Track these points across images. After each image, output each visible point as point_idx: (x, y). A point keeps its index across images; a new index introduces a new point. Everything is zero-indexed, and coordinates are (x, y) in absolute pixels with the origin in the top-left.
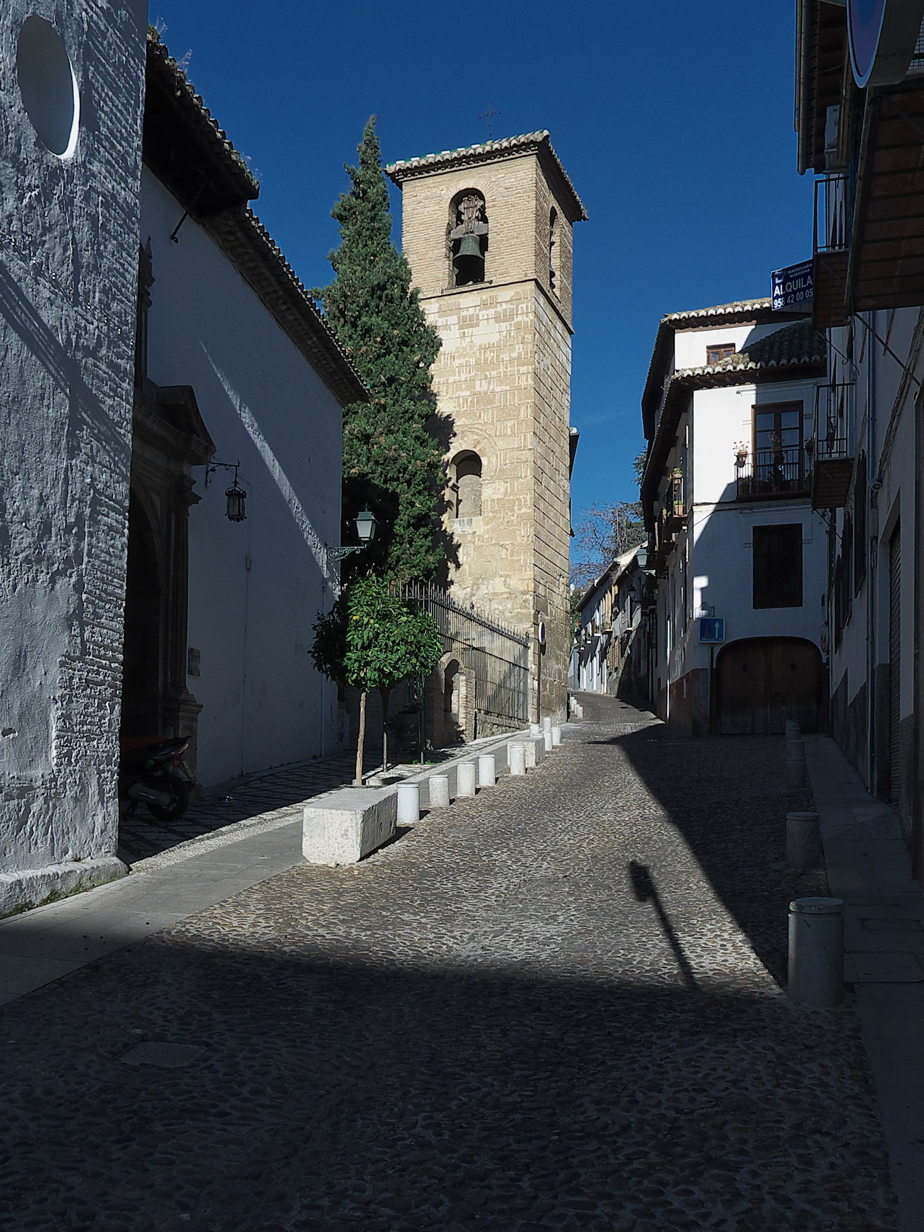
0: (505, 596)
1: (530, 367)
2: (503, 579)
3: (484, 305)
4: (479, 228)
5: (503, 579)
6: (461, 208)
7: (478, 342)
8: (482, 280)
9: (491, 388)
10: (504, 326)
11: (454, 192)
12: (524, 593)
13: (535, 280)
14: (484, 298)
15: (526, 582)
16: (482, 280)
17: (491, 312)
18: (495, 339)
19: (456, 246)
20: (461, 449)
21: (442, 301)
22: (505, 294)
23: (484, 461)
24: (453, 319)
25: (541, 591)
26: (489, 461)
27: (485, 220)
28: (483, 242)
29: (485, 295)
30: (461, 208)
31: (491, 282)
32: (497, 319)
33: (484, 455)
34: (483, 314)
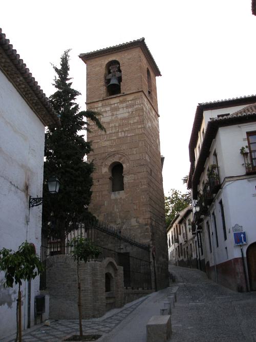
0: (137, 227)
2: (135, 219)
3: (121, 102)
4: (118, 74)
5: (135, 219)
6: (110, 68)
7: (119, 116)
8: (120, 93)
9: (126, 135)
10: (130, 110)
11: (107, 62)
12: (146, 225)
16: (120, 93)
17: (124, 105)
18: (126, 115)
19: (108, 81)
20: (113, 161)
21: (104, 102)
22: (130, 98)
23: (124, 166)
24: (108, 109)
25: (154, 223)
26: (126, 166)
27: (120, 71)
28: (120, 79)
29: (121, 99)
30: (110, 68)
31: (124, 93)
32: (127, 107)
33: (124, 163)
34: (121, 106)
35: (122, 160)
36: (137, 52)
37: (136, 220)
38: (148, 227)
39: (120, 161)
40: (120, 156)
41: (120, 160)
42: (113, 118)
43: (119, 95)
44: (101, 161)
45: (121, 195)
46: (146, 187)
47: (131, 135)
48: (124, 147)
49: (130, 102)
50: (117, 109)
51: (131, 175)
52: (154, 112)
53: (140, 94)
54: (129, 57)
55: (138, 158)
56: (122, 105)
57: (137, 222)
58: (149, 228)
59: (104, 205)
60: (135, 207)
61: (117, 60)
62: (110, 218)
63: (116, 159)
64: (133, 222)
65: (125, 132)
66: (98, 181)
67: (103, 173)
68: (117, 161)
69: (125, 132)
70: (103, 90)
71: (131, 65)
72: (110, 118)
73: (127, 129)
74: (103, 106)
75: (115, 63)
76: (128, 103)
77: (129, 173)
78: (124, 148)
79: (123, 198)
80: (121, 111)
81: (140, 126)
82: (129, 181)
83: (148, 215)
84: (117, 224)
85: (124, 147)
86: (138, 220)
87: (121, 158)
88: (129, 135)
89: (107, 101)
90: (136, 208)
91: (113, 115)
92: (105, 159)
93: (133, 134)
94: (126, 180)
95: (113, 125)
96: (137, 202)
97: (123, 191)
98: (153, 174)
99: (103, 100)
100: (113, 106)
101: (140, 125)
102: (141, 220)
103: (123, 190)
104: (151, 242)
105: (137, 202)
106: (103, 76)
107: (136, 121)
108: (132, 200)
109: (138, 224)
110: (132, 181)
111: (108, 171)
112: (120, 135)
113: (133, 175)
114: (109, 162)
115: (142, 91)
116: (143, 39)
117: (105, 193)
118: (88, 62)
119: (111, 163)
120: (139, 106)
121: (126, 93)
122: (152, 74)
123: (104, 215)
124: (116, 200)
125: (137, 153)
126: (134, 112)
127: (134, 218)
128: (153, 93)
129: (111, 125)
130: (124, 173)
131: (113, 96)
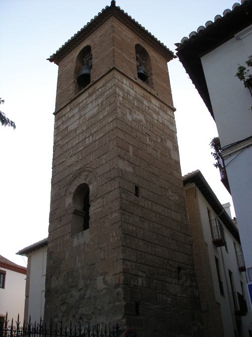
0: (104, 291)
3: (90, 95)
7: (87, 116)
10: (100, 101)
11: (78, 52)
12: (117, 286)
14: (90, 91)
15: (118, 276)
17: (94, 97)
18: (95, 111)
20: (78, 184)
21: (71, 105)
23: (91, 187)
24: (76, 110)
29: (90, 90)
33: (90, 183)
35: (87, 181)
37: (104, 279)
38: (120, 289)
40: (86, 174)
41: (86, 180)
42: (81, 121)
44: (65, 189)
46: (117, 215)
47: (100, 136)
49: (100, 90)
50: (84, 107)
51: (98, 201)
52: (154, 101)
53: (111, 73)
54: (101, 34)
56: (91, 98)
57: (105, 282)
62: (70, 280)
64: (100, 284)
65: (92, 135)
66: (61, 220)
67: (66, 207)
68: (83, 182)
71: (103, 42)
72: (77, 122)
73: (95, 130)
74: (71, 109)
75: (88, 49)
78: (91, 160)
79: (87, 242)
81: (111, 119)
82: (96, 211)
83: (119, 268)
84: (80, 290)
86: (106, 277)
87: (87, 176)
88: (98, 138)
89: (75, 102)
90: (103, 257)
93: (103, 135)
96: (105, 245)
97: (88, 230)
98: (142, 192)
100: (81, 105)
104: (124, 321)
105: (105, 245)
107: (106, 113)
108: (98, 243)
109: (106, 286)
111: (71, 203)
112: (87, 142)
113: (101, 200)
114: (73, 189)
117: (68, 237)
118: (61, 63)
119: (75, 188)
120: (111, 91)
122: (152, 53)
123: (65, 276)
126: (104, 102)
127: (101, 275)
128: (155, 78)
129: (78, 132)
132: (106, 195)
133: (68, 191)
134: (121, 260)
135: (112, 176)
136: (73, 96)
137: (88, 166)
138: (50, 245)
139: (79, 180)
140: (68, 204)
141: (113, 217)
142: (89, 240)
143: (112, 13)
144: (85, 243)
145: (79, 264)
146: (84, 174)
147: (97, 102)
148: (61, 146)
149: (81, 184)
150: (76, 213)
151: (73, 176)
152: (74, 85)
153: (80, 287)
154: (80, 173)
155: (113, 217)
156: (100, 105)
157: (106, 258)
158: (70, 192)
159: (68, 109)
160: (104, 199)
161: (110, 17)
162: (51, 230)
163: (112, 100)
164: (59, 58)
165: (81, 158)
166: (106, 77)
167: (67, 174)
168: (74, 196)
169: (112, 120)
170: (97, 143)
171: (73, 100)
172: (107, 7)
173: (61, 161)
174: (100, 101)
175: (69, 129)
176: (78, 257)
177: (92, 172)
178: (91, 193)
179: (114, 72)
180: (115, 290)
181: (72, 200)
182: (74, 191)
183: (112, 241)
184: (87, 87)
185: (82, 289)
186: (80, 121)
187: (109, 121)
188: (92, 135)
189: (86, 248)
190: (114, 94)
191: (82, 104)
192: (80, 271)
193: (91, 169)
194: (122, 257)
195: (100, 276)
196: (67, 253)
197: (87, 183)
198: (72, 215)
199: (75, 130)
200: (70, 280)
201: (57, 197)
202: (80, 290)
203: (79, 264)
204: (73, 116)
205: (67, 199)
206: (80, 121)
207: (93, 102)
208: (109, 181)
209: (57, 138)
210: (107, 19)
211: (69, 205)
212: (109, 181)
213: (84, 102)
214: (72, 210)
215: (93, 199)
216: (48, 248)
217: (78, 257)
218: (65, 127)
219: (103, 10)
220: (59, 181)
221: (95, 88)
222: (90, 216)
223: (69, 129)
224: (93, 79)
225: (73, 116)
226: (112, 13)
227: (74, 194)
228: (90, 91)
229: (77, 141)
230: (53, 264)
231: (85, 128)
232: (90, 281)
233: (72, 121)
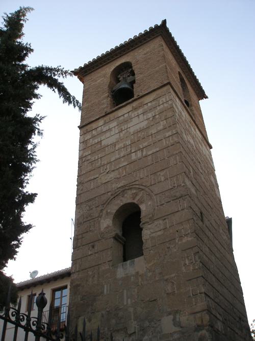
0: (176, 336)
1: (174, 131)
2: (171, 317)
3: (135, 109)
5: (171, 317)
7: (132, 130)
10: (150, 115)
12: (199, 328)
13: (169, 83)
15: (199, 315)
17: (140, 111)
20: (122, 204)
21: (105, 118)
23: (143, 207)
25: (219, 326)
29: (135, 104)
30: (119, 76)
33: (142, 203)
34: (133, 115)
35: (138, 198)
36: (158, 43)
37: (174, 320)
38: (204, 332)
39: (135, 201)
40: (135, 191)
43: (133, 99)
44: (99, 209)
45: (139, 265)
46: (190, 239)
47: (155, 151)
48: (142, 174)
49: (149, 104)
51: (156, 223)
53: (165, 89)
54: (145, 52)
55: (170, 187)
56: (136, 113)
57: (176, 323)
58: (207, 334)
59: (102, 292)
60: (169, 288)
61: (128, 61)
62: (113, 321)
63: (127, 199)
66: (93, 247)
68: (130, 201)
69: (142, 150)
70: (106, 102)
71: (149, 59)
72: (117, 136)
73: (145, 144)
74: (105, 124)
75: (127, 66)
76: (146, 107)
77: (152, 220)
80: (135, 121)
82: (154, 235)
84: (130, 335)
85: (142, 174)
86: (178, 316)
87: (136, 194)
88: (150, 153)
89: (112, 116)
90: (170, 291)
91: (122, 131)
92: (108, 203)
93: (158, 149)
94: (147, 233)
95: (121, 145)
96: (173, 275)
97: (142, 258)
99: (106, 115)
101: (169, 131)
102: (184, 319)
103: (141, 254)
105: (173, 275)
106: (106, 87)
107: (161, 127)
108: (160, 273)
109: (178, 329)
110: (159, 233)
111: (111, 225)
113: (161, 222)
114: (114, 208)
115: (169, 83)
116: (164, 22)
118: (87, 78)
120: (166, 105)
121: (141, 94)
123: (103, 316)
124: (126, 279)
125: (166, 179)
126: (157, 116)
127: (170, 314)
129: (117, 148)
130: (143, 220)
131: (121, 105)
132: (169, 216)
133: (104, 212)
134: (203, 295)
135: (178, 194)
136: (109, 110)
137: (137, 183)
138: (74, 276)
139: (122, 198)
140: (105, 225)
141: (184, 241)
142: (145, 269)
143: (161, 32)
144: (137, 273)
145: (129, 300)
146: (130, 192)
147: (145, 116)
148: (90, 161)
149: (126, 204)
150: (116, 238)
151: (112, 195)
152: (109, 99)
153: (130, 331)
154: (124, 191)
155: (184, 241)
156: (151, 119)
157: (176, 292)
158: (107, 213)
159: (101, 122)
160: (167, 220)
161: (157, 36)
162: (75, 259)
163: (170, 114)
164: (86, 72)
165: (124, 174)
166: (159, 92)
167: (103, 192)
168: (114, 218)
169: (171, 134)
170: (149, 158)
171: (109, 114)
172: (156, 26)
173: (93, 178)
174: (150, 115)
175: (103, 144)
176: (125, 291)
177: (143, 190)
178: (143, 214)
179: (169, 86)
180: (196, 333)
181: (111, 222)
182: (114, 211)
183: (185, 271)
184: (130, 101)
185: (135, 333)
186: (120, 135)
187: (167, 136)
188: (142, 150)
189: (140, 280)
190: (171, 108)
191: (122, 118)
192: (131, 310)
193: (141, 187)
194: (203, 290)
195: (167, 316)
196: (105, 286)
197: (136, 203)
198: (112, 240)
199: (114, 144)
200: (113, 321)
201: (87, 218)
202: (130, 335)
203: (129, 300)
204: (110, 130)
205: (102, 221)
206: (120, 135)
207: (140, 116)
208: (173, 200)
209: (84, 153)
210: (153, 38)
211: (107, 228)
212: (173, 200)
213: (126, 116)
214: (113, 234)
215: (148, 220)
216: (72, 280)
217: (125, 291)
218: (96, 141)
219: (151, 29)
220: (89, 201)
221: (141, 103)
222: (144, 241)
223: (103, 143)
224: (137, 91)
225: (110, 130)
226: (161, 32)
227: (115, 215)
228: (134, 106)
229: (117, 156)
230: (81, 300)
231: (128, 142)
232: (149, 322)
233: (108, 134)
